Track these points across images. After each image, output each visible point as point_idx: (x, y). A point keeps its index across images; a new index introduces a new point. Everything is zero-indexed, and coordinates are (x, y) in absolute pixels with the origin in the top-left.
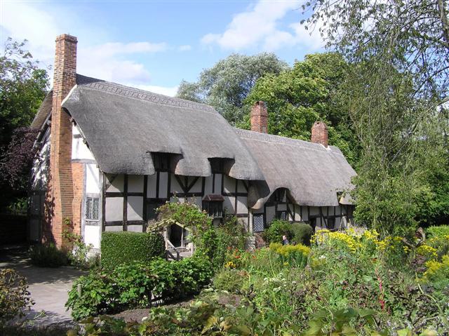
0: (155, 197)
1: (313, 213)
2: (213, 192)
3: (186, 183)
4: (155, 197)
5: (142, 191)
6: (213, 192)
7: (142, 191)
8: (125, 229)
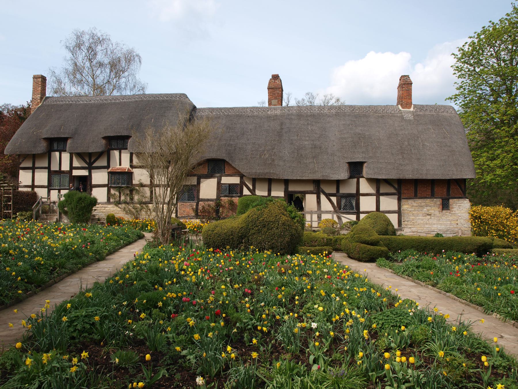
0: (58, 169)
1: (292, 188)
2: (120, 165)
3: (90, 160)
4: (58, 169)
5: (47, 166)
6: (120, 165)
7: (47, 166)
8: (33, 189)
